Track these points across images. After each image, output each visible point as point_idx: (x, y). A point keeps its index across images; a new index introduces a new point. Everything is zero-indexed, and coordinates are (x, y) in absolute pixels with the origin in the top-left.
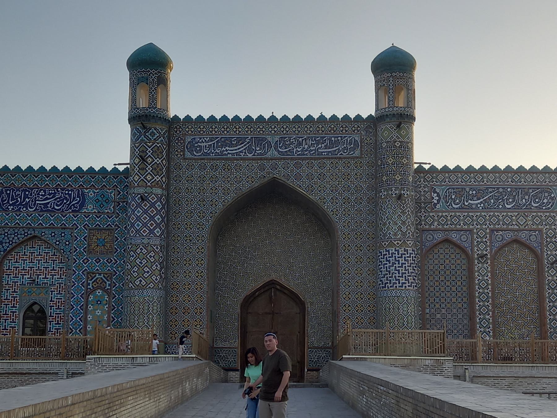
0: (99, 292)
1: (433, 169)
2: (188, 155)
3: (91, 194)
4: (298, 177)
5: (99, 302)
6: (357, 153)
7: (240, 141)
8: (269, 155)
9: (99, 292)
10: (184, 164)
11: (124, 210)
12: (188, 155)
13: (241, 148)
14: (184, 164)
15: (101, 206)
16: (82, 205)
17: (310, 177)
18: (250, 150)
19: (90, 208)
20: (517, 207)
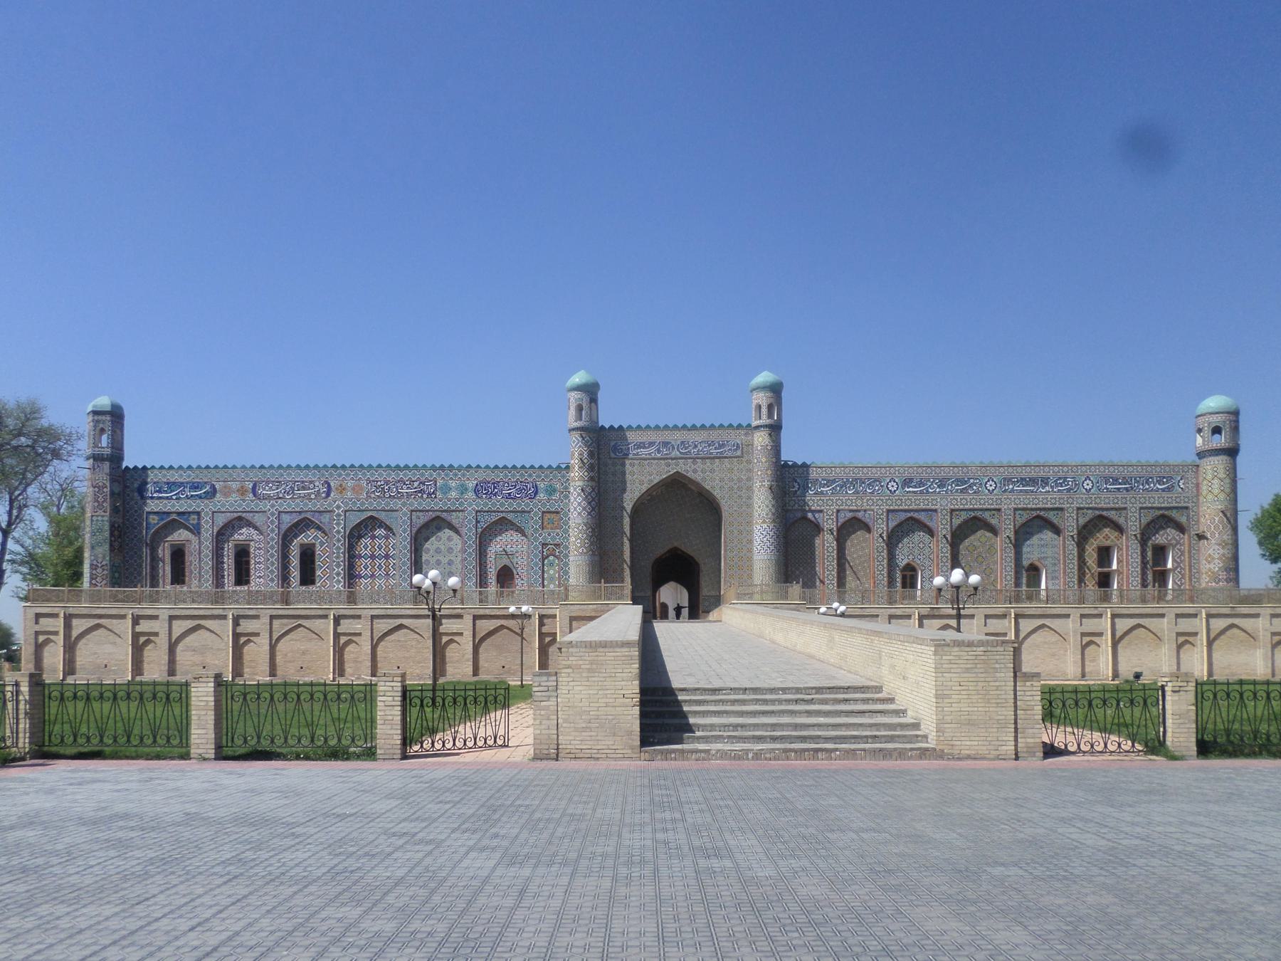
0: (551, 558)
1: (795, 465)
2: (613, 455)
3: (541, 485)
4: (695, 471)
5: (551, 564)
6: (739, 453)
7: (651, 444)
8: (673, 455)
9: (551, 558)
10: (610, 462)
11: (567, 497)
12: (613, 455)
13: (652, 449)
14: (610, 462)
15: (550, 494)
16: (536, 493)
17: (703, 471)
18: (659, 451)
19: (541, 496)
20: (857, 492)
